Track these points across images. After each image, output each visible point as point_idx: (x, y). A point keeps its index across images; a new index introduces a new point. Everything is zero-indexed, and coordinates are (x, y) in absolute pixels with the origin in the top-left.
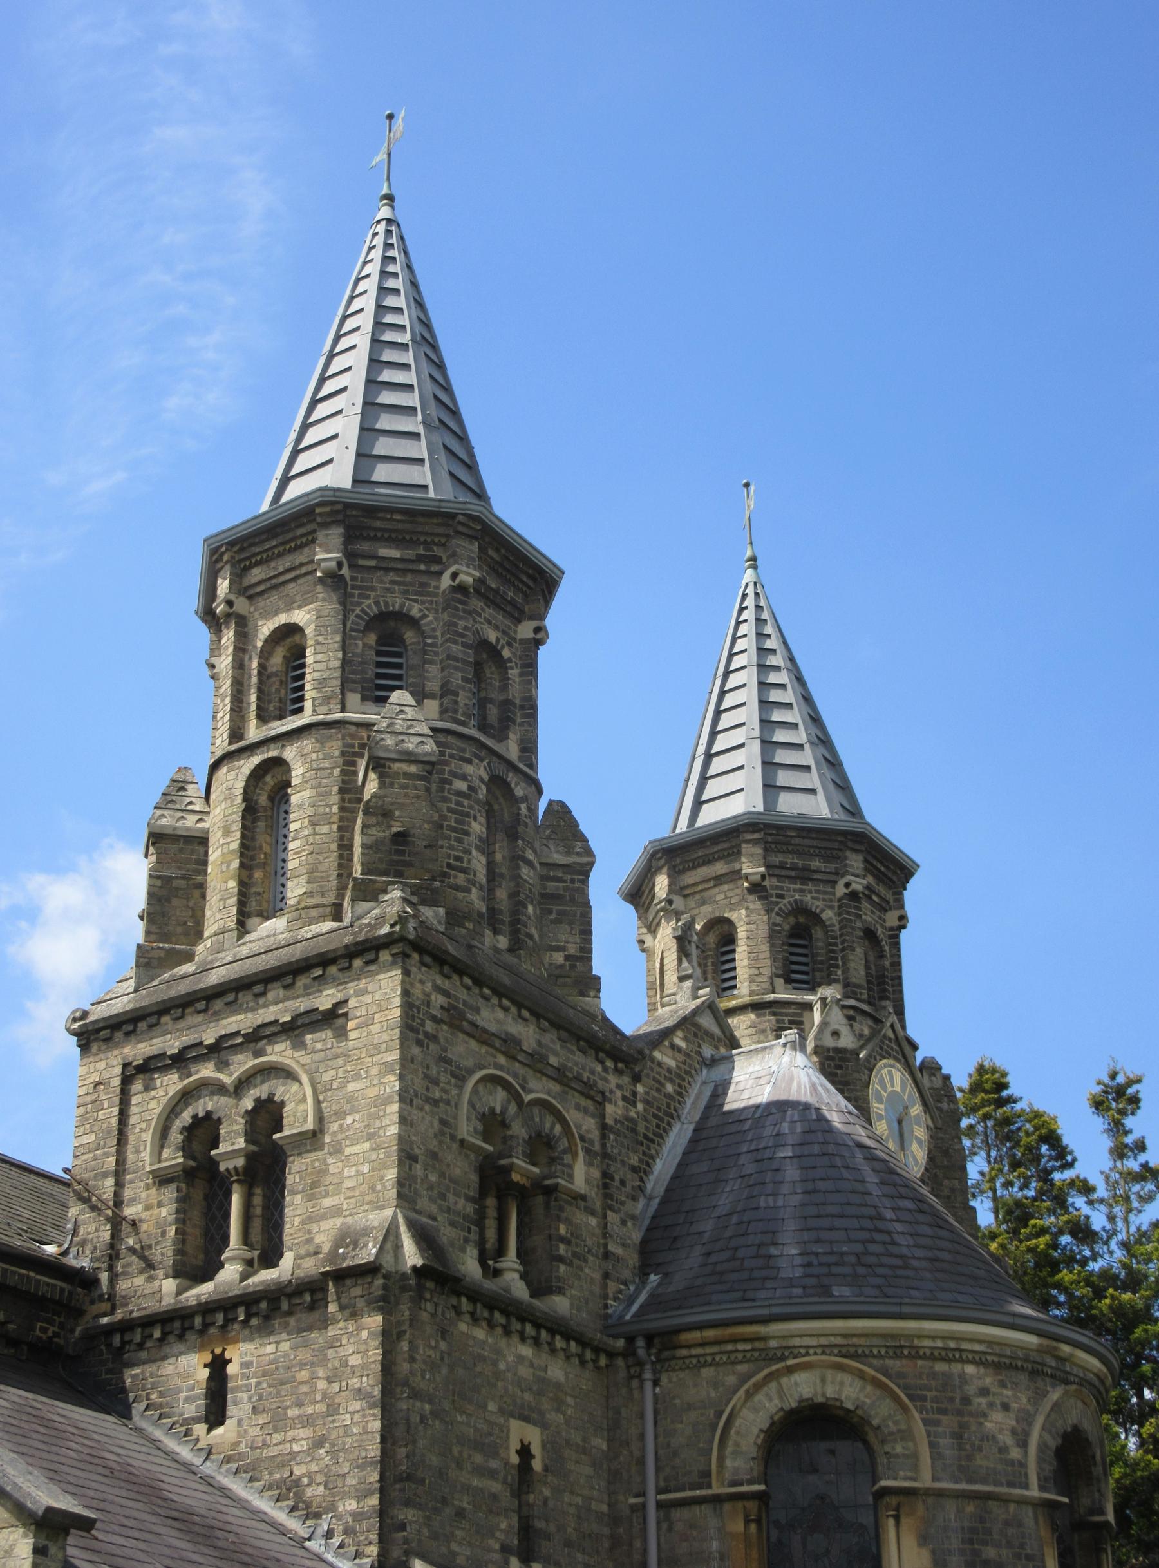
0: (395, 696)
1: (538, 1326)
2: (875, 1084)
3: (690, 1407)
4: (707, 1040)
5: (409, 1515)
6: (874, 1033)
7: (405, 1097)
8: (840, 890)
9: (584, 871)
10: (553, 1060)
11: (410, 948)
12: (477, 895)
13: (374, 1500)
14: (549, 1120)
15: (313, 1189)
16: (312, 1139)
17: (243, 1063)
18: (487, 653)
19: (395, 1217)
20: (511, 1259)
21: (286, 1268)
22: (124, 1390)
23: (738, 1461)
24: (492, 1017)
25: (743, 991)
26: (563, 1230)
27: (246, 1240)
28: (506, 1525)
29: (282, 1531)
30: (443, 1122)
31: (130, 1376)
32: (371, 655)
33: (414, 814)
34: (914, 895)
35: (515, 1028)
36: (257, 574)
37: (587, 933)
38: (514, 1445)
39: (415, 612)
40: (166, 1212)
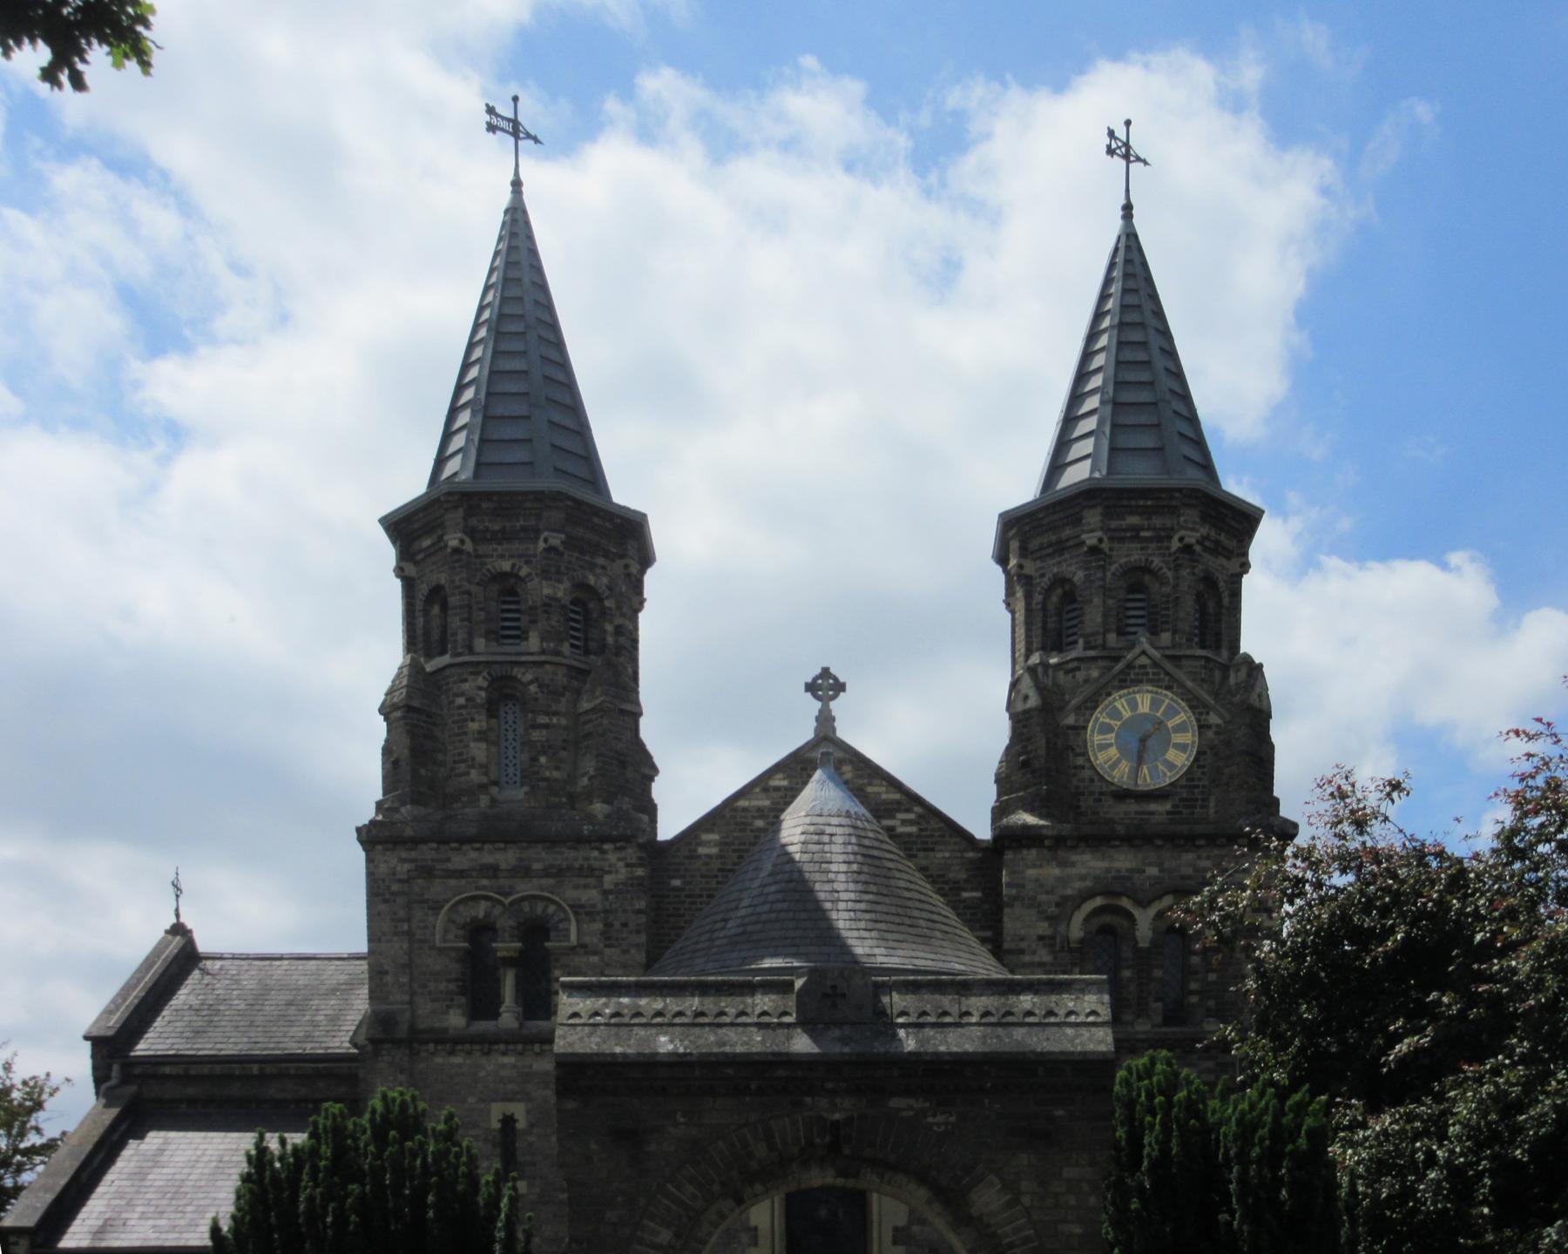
10: (537, 866)
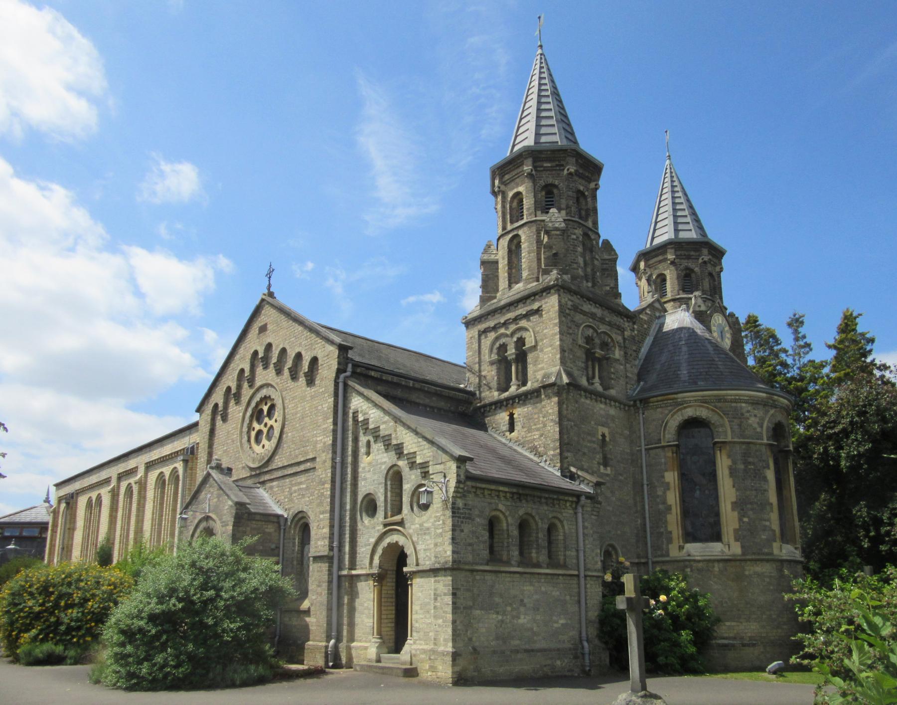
0: (552, 210)
1: (606, 399)
2: (713, 321)
3: (654, 420)
4: (657, 310)
5: (569, 454)
6: (712, 305)
7: (561, 333)
8: (700, 261)
9: (614, 261)
10: (607, 319)
11: (560, 288)
12: (581, 269)
13: (558, 451)
14: (607, 337)
15: (536, 362)
16: (534, 348)
17: (513, 327)
18: (580, 195)
19: (560, 370)
20: (597, 380)
21: (529, 386)
22: (485, 424)
23: (669, 435)
24: (587, 307)
25: (669, 296)
26: (612, 370)
27: (517, 378)
28: (599, 457)
29: (532, 460)
30: (573, 340)
31: (487, 420)
32: (544, 198)
33: (559, 246)
34: (725, 261)
35: (594, 310)
36: (507, 177)
37: (616, 280)
38: (600, 433)
39: (556, 183)
40: (494, 373)
